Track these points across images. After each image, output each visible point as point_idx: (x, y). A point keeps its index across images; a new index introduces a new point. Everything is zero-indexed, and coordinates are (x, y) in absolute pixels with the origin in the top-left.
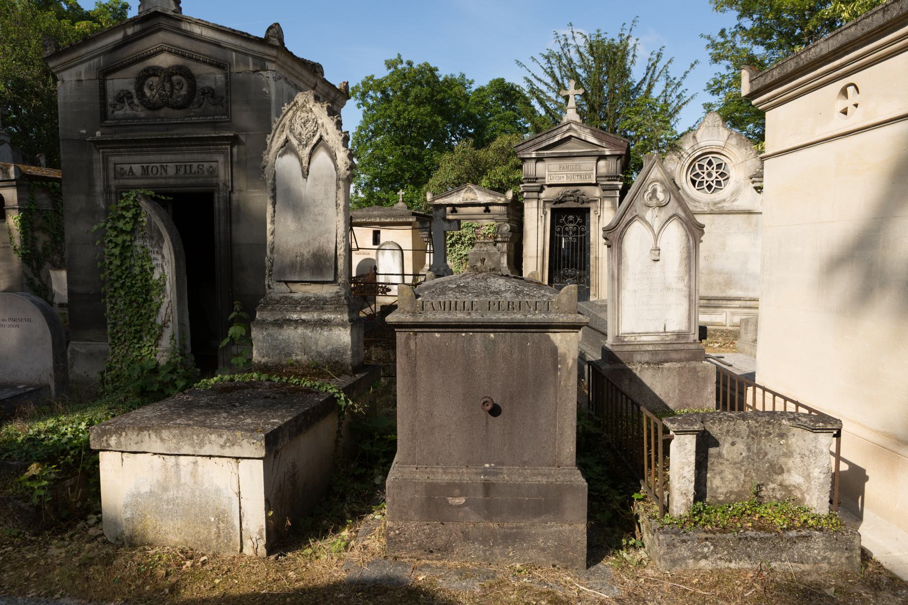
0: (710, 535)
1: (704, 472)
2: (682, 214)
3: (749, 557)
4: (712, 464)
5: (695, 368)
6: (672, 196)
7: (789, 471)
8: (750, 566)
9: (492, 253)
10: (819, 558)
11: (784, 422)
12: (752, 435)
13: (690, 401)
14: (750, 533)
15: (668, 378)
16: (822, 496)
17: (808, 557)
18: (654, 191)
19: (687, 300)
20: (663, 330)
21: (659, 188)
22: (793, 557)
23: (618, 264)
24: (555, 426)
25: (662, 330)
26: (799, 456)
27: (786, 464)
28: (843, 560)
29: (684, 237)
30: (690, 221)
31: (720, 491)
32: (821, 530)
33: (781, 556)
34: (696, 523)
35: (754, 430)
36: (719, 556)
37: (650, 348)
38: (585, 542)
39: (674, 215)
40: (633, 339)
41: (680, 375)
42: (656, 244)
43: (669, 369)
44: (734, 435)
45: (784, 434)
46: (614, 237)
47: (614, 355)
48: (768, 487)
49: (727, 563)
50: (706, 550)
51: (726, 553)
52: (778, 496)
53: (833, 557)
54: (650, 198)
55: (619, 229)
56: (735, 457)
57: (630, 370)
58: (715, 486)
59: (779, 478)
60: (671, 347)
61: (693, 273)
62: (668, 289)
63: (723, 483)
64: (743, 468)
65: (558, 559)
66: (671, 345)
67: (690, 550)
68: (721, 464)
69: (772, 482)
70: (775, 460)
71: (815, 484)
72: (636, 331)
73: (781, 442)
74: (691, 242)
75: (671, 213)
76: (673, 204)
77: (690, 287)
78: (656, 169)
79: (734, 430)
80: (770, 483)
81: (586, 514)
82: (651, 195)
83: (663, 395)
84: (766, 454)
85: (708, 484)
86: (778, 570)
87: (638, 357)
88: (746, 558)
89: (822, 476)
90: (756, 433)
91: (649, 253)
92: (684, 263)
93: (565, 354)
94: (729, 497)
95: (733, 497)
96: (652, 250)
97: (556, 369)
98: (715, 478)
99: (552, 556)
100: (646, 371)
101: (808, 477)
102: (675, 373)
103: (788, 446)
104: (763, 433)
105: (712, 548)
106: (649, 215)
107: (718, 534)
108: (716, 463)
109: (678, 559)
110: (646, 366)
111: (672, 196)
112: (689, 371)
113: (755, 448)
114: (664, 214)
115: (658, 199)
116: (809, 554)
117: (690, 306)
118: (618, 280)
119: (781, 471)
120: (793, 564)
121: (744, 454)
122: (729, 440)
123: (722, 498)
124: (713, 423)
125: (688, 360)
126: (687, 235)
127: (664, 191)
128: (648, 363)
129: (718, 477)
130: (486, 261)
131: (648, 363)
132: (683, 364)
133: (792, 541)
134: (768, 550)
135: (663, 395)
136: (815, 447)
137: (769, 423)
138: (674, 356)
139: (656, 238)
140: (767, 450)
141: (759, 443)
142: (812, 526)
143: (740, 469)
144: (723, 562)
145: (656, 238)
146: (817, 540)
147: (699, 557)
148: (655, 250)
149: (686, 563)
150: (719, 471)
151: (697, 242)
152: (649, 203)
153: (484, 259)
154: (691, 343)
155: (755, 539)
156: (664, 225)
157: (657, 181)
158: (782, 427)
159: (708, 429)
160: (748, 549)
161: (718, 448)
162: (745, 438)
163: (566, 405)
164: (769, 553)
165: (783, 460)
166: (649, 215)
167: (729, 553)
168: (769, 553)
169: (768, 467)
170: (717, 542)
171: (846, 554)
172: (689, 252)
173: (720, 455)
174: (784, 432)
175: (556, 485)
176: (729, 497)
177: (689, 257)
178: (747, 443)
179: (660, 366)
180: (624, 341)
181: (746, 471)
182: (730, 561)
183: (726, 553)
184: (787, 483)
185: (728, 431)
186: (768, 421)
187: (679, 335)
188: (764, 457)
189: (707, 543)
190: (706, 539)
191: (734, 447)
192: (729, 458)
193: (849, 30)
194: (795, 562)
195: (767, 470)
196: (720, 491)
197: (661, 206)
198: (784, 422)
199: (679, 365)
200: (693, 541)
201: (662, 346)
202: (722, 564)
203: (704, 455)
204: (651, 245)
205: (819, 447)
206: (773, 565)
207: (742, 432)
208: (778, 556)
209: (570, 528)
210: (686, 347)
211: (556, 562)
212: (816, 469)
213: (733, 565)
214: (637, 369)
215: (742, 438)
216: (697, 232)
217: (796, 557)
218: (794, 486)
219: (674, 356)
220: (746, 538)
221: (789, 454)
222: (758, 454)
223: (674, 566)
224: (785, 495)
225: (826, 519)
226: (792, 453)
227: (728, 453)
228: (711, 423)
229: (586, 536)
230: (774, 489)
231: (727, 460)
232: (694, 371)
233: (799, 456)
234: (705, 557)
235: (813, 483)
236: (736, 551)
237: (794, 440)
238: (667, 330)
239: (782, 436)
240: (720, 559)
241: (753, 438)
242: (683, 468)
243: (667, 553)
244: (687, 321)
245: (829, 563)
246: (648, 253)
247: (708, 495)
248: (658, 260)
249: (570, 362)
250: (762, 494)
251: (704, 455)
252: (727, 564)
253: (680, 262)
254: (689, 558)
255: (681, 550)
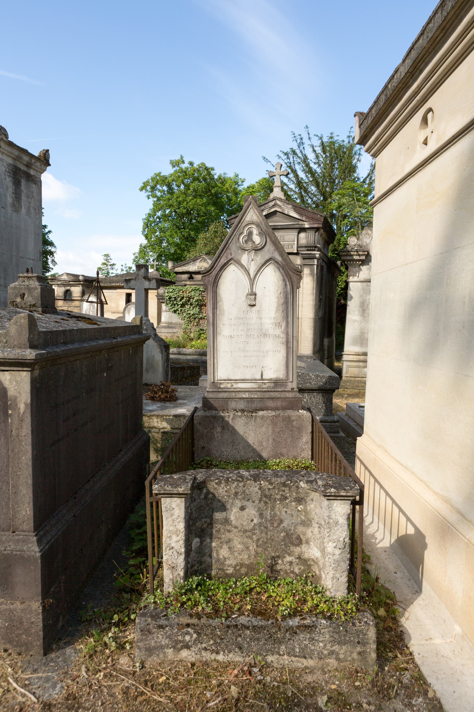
0: (194, 621)
1: (208, 540)
2: (279, 258)
3: (240, 648)
4: (218, 531)
5: (289, 417)
6: (268, 240)
7: (307, 542)
8: (241, 659)
9: (32, 288)
10: (326, 652)
11: (301, 483)
12: (264, 499)
13: (284, 451)
14: (243, 620)
15: (261, 427)
16: (338, 576)
17: (312, 651)
18: (250, 234)
19: (285, 346)
20: (260, 378)
21: (255, 231)
22: (294, 650)
23: (213, 309)
24: (8, 483)
25: (259, 377)
26: (317, 526)
27: (304, 534)
28: (355, 655)
29: (281, 282)
30: (287, 265)
31: (228, 562)
32: (330, 618)
33: (279, 648)
34: (183, 604)
35: (267, 493)
36: (204, 645)
37: (246, 395)
38: (41, 624)
39: (270, 259)
40: (229, 385)
41: (274, 424)
42: (252, 288)
43: (262, 417)
44: (244, 498)
45: (302, 499)
46: (209, 281)
47: (209, 401)
48: (285, 560)
49: (214, 655)
50: (187, 638)
51: (211, 642)
52: (297, 571)
53: (342, 652)
54: (245, 241)
55: (214, 273)
56: (245, 523)
57: (223, 418)
58: (221, 557)
59: (297, 550)
60: (267, 395)
61: (290, 319)
62: (265, 335)
63: (232, 553)
64: (254, 537)
65: (10, 642)
66: (268, 393)
67: (169, 637)
68: (229, 531)
69: (289, 555)
70: (292, 528)
71: (329, 560)
72: (233, 378)
73: (299, 508)
74: (288, 287)
75: (267, 257)
76: (270, 247)
77: (287, 334)
78: (251, 211)
79: (244, 492)
80: (287, 556)
81: (40, 590)
82: (246, 238)
83: (256, 443)
84: (281, 521)
85: (214, 554)
86: (275, 665)
87: (233, 405)
88: (237, 650)
89: (338, 552)
90: (269, 497)
91: (245, 297)
92: (281, 309)
93: (16, 398)
94: (239, 570)
95: (243, 571)
96: (248, 295)
97: (6, 415)
98: (221, 547)
99: (3, 638)
100: (239, 419)
101: (323, 551)
102: (268, 422)
103: (306, 513)
104: (278, 497)
105: (195, 636)
106: (245, 259)
107: (204, 620)
108: (222, 531)
109: (155, 648)
110: (240, 414)
111: (268, 240)
112: (283, 420)
113: (268, 514)
114: (260, 258)
115: (254, 242)
116: (313, 648)
117: (287, 353)
118: (213, 325)
119: (299, 542)
120: (294, 659)
121: (255, 521)
122: (238, 503)
123: (230, 571)
124: (219, 484)
125: (284, 409)
126: (284, 280)
127: (260, 234)
128: (243, 411)
129: (225, 546)
130: (26, 296)
131: (243, 411)
132: (278, 412)
133: (293, 631)
134: (263, 641)
135: (256, 443)
136: (329, 517)
137: (284, 485)
138: (271, 404)
139: (252, 282)
140: (282, 517)
141: (273, 508)
142: (322, 612)
143: (252, 539)
144: (209, 653)
145: (252, 282)
146: (322, 631)
147: (179, 646)
148: (251, 295)
149: (164, 653)
150: (227, 539)
151: (295, 288)
152: (245, 245)
153: (24, 294)
154: (288, 391)
155: (248, 628)
156: (260, 269)
157: (253, 223)
158: (300, 490)
159: (212, 490)
160: (239, 639)
161: (224, 513)
162: (257, 502)
163: (19, 458)
164: (265, 644)
165: (300, 529)
166: (245, 259)
167: (216, 643)
168: (265, 644)
169: (284, 537)
170: (202, 629)
171: (359, 649)
172: (286, 298)
173: (227, 521)
174: (302, 496)
175: (3, 554)
176: (239, 570)
177: (286, 303)
178: (259, 508)
179: (254, 414)
180: (220, 388)
181: (258, 540)
182: (218, 653)
183: (211, 642)
184: (306, 556)
185: (236, 494)
186: (284, 483)
187: (277, 382)
188: (279, 525)
189: (189, 630)
190: (188, 625)
191: (244, 513)
192: (238, 524)
193: (418, 43)
194: (296, 656)
195: (283, 541)
196: (228, 562)
197: (257, 250)
198: (301, 483)
199: (274, 413)
200: (172, 627)
201: (259, 393)
202: (207, 656)
203: (208, 521)
204: (247, 290)
205: (333, 516)
206: (270, 658)
207: (254, 494)
208: (275, 648)
209: (22, 606)
210: (283, 395)
211: (8, 646)
212: (330, 543)
213: (220, 657)
214: (229, 416)
215: (254, 502)
216: (295, 278)
217: (297, 650)
218: (313, 560)
219: (271, 404)
220: (236, 626)
221: (307, 523)
222: (272, 521)
223: (150, 656)
224: (304, 571)
225: (340, 603)
226: (311, 521)
227: (237, 519)
228: (216, 483)
229: (41, 616)
230: (291, 563)
231: (236, 527)
232: (288, 420)
233: (317, 526)
234: (187, 647)
235: (327, 559)
236: (224, 641)
237: (312, 506)
238: (264, 377)
239: (300, 500)
240: (205, 649)
241: (266, 502)
242: (170, 537)
243: (141, 640)
244: (285, 368)
245: (338, 659)
246: (244, 298)
247: (213, 567)
248: (254, 305)
249: (22, 407)
250: (278, 567)
251: (208, 521)
252: (213, 656)
253: (277, 308)
254: (167, 646)
255: (158, 637)
